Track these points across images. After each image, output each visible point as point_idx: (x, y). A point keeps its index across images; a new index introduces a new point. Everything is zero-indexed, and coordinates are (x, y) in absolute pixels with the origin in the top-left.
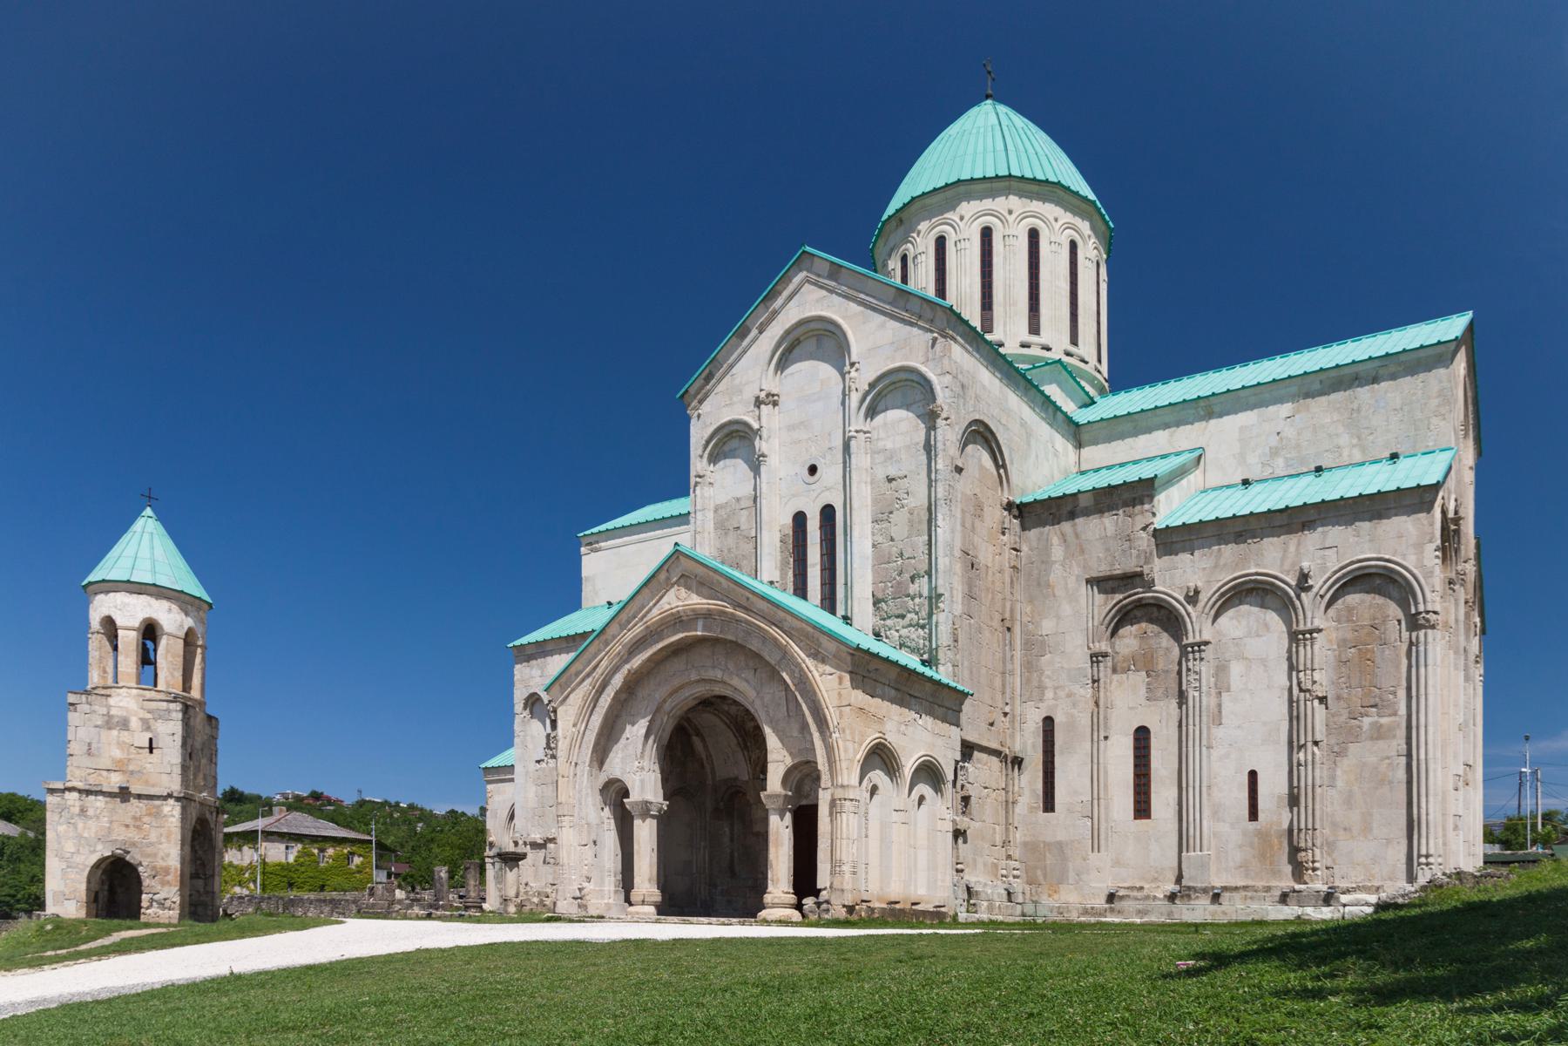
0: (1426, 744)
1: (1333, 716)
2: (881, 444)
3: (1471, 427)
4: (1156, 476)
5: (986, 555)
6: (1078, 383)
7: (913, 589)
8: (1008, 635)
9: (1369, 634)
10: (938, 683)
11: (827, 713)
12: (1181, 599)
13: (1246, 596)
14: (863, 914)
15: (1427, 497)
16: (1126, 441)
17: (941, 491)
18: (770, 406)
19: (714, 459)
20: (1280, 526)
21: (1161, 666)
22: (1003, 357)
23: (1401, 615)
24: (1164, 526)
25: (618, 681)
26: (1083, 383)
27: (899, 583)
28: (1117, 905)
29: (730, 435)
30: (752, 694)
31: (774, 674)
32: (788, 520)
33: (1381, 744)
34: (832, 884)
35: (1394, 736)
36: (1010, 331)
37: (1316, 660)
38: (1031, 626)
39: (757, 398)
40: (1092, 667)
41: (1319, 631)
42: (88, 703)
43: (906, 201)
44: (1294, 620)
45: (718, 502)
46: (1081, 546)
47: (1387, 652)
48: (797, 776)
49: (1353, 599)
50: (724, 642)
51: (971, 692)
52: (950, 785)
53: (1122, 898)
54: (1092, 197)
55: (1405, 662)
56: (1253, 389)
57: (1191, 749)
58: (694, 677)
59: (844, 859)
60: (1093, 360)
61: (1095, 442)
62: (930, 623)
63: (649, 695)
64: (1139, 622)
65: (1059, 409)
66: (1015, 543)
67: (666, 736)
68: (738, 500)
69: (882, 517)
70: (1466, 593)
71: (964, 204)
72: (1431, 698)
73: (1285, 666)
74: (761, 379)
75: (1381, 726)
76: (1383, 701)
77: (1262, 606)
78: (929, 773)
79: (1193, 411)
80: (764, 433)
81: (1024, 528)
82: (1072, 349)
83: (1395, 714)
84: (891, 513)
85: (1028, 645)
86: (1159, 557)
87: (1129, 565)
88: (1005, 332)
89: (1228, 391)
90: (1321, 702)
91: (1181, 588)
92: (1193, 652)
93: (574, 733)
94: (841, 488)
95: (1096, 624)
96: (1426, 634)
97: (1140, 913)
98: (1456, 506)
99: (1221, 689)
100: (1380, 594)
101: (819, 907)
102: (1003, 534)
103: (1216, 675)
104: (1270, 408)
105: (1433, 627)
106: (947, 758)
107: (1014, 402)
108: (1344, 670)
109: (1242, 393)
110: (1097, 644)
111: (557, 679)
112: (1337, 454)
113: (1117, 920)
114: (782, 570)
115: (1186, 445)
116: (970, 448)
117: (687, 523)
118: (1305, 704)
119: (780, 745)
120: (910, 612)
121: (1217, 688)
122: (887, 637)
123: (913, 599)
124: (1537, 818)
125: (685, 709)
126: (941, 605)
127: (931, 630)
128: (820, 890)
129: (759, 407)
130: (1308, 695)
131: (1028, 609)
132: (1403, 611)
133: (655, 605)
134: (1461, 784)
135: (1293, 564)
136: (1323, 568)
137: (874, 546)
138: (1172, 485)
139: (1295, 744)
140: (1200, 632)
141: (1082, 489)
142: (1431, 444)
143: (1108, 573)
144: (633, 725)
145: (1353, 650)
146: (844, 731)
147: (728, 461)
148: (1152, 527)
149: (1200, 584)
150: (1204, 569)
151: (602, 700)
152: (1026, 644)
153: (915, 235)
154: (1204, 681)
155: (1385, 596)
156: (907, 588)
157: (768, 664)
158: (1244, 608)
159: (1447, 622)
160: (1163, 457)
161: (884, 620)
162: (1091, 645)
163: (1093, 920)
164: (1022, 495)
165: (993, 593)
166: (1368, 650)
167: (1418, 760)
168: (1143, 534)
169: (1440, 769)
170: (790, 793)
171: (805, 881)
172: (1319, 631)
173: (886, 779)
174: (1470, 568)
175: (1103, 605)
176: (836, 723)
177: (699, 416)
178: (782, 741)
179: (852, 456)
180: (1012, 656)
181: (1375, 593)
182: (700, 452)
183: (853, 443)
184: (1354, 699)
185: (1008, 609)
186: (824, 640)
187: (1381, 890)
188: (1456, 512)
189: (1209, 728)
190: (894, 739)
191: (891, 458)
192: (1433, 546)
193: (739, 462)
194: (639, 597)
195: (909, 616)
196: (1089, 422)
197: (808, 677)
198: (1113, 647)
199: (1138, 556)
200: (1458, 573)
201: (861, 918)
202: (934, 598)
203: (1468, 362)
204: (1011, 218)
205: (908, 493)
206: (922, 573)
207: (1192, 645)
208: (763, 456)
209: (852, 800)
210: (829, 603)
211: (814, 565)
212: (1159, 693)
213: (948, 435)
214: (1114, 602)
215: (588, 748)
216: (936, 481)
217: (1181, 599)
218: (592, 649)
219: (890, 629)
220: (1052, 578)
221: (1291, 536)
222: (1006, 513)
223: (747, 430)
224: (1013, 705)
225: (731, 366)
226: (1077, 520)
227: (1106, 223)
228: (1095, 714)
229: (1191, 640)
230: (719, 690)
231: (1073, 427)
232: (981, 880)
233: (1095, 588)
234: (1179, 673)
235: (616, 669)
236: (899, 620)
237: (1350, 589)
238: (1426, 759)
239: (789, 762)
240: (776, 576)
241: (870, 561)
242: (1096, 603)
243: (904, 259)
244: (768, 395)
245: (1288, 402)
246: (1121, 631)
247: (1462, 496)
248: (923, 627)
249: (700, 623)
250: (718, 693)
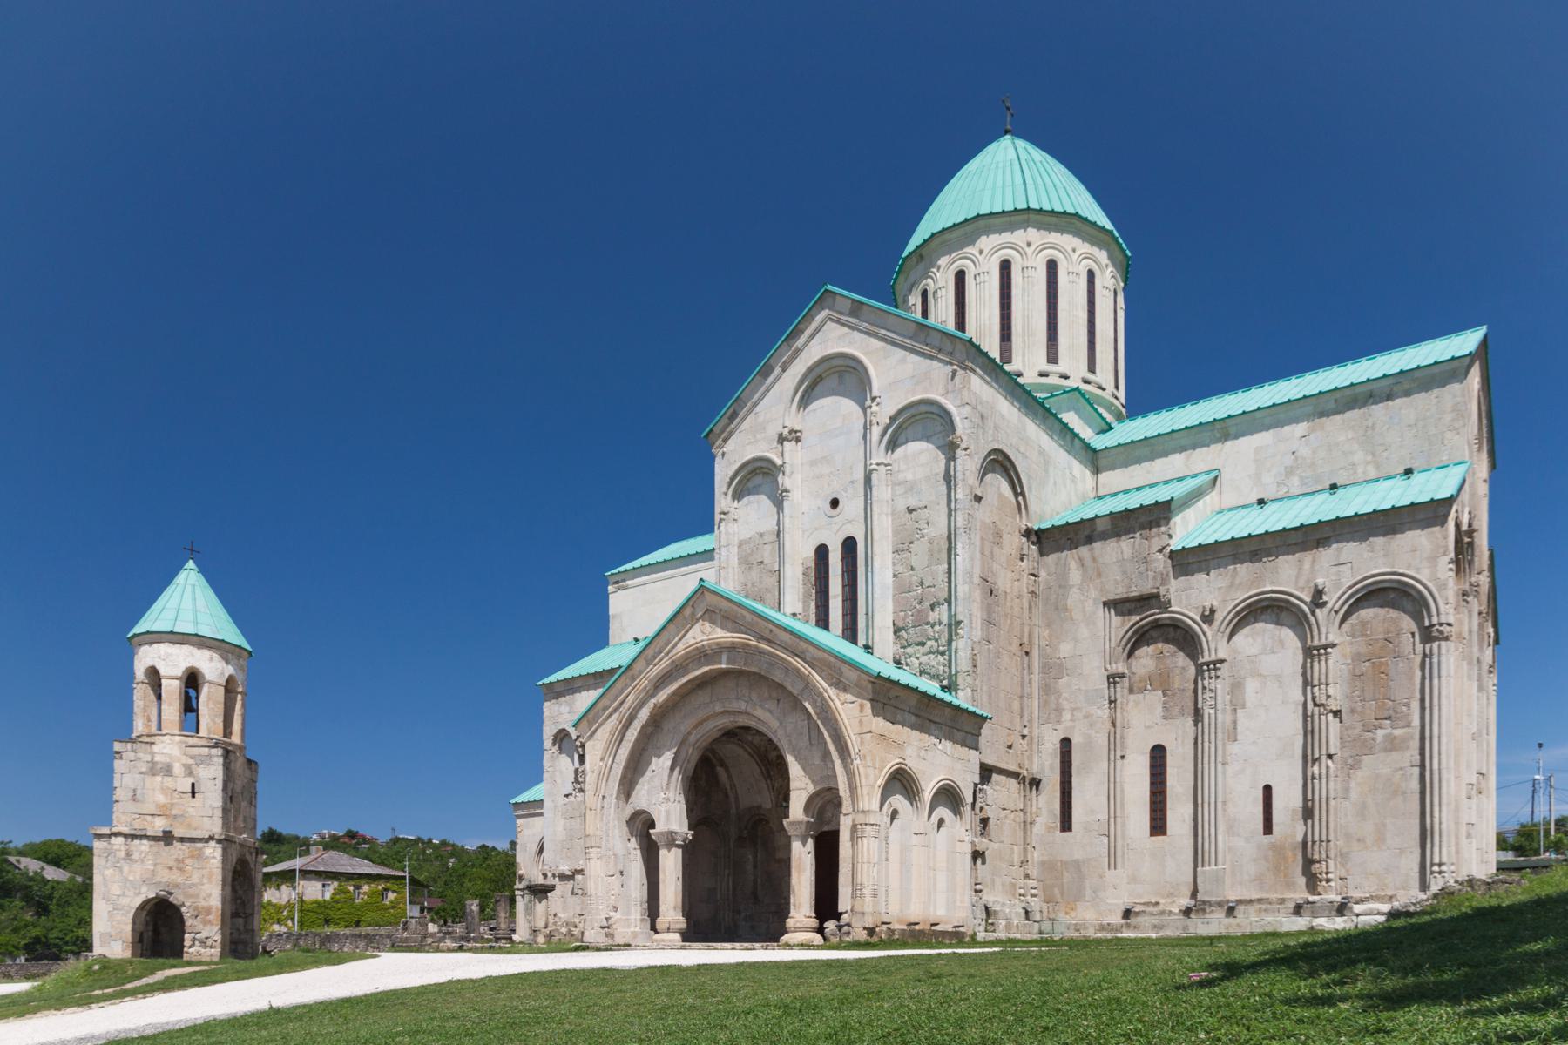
0: (1439, 754)
1: (1347, 729)
2: (901, 477)
3: (1485, 440)
4: (1172, 498)
5: (1004, 581)
6: (1096, 410)
7: (933, 617)
8: (1026, 658)
9: (1382, 648)
10: (958, 708)
11: (849, 741)
12: (1197, 618)
13: (1262, 612)
14: (883, 936)
15: (1441, 511)
16: (1143, 465)
17: (960, 520)
18: (793, 442)
19: (738, 495)
20: (1295, 544)
21: (1177, 685)
22: (1022, 386)
23: (1415, 628)
24: (1180, 548)
25: (644, 715)
26: (1101, 410)
27: (919, 611)
28: (1133, 921)
29: (754, 472)
30: (775, 724)
31: (797, 704)
32: (810, 553)
33: (1395, 755)
34: (853, 907)
35: (1408, 748)
36: (1028, 362)
37: (1331, 675)
38: (1049, 650)
39: (781, 435)
40: (1109, 688)
41: (1334, 646)
43: (926, 237)
44: (1309, 636)
45: (742, 538)
46: (1098, 569)
47: (1401, 665)
48: (818, 803)
49: (1367, 613)
50: (749, 673)
51: (990, 716)
52: (969, 808)
53: (1138, 913)
54: (1109, 226)
55: (1418, 674)
56: (1267, 410)
57: (1206, 766)
58: (718, 709)
59: (865, 882)
60: (1110, 387)
61: (1113, 468)
62: (949, 650)
63: (674, 728)
64: (1155, 642)
65: (1077, 436)
66: (1034, 568)
67: (692, 766)
68: (761, 535)
69: (902, 547)
70: (1480, 605)
71: (983, 238)
72: (1444, 709)
73: (1300, 681)
74: (784, 416)
75: (1395, 738)
76: (1397, 713)
77: (1278, 623)
78: (948, 796)
79: (1209, 434)
80: (787, 469)
81: (1042, 554)
82: (1090, 377)
83: (1408, 726)
84: (911, 543)
85: (1046, 668)
86: (1175, 578)
87: (1146, 587)
88: (1023, 362)
89: (1244, 412)
90: (1335, 716)
91: (1197, 608)
92: (1209, 670)
93: (601, 766)
94: (863, 520)
95: (1113, 645)
96: (1439, 646)
97: (1156, 927)
98: (1470, 519)
99: (1236, 705)
100: (1393, 607)
101: (840, 930)
102: (1022, 560)
103: (1231, 693)
104: (1285, 428)
105: (1446, 639)
106: (966, 781)
107: (1033, 430)
108: (1357, 683)
109: (1258, 415)
110: (1114, 666)
111: (585, 715)
112: (1351, 472)
113: (1132, 935)
114: (804, 602)
115: (1202, 467)
116: (989, 476)
117: (712, 559)
118: (1320, 719)
119: (802, 773)
120: (930, 639)
121: (1232, 705)
122: (907, 665)
123: (932, 627)
124: (1549, 824)
125: (710, 740)
126: (960, 631)
127: (950, 656)
128: (841, 914)
129: (782, 444)
130: (1322, 709)
131: (1046, 633)
132: (1417, 623)
133: (680, 640)
134: (1474, 793)
135: (1308, 581)
136: (1338, 584)
137: (895, 576)
138: (1189, 507)
139: (1309, 758)
140: (1216, 650)
141: (1100, 514)
142: (1445, 458)
143: (1125, 596)
144: (659, 758)
145: (1367, 664)
146: (865, 756)
147: (751, 498)
148: (1168, 550)
149: (1215, 604)
150: (1220, 588)
151: (628, 734)
152: (1044, 667)
153: (935, 270)
154: (1219, 698)
155: (1398, 609)
156: (927, 616)
157: (790, 694)
158: (1260, 625)
159: (1460, 634)
160: (1180, 479)
161: (904, 647)
162: (1108, 667)
163: (1109, 936)
164: (1040, 522)
165: (1011, 619)
166: (1382, 663)
167: (1431, 770)
168: (1160, 556)
169: (1453, 778)
170: (812, 820)
171: (826, 906)
172: (1334, 646)
173: (907, 803)
174: (1484, 580)
175: (1119, 627)
176: (857, 750)
177: (723, 454)
178: (804, 769)
179: (874, 489)
180: (1031, 679)
181: (1388, 606)
182: (724, 490)
183: (874, 476)
184: (1368, 712)
185: (1026, 635)
186: (845, 669)
187: (1394, 899)
188: (1470, 525)
189: (1224, 745)
190: (914, 765)
191: (911, 489)
192: (1447, 559)
193: (763, 498)
194: (665, 633)
195: (929, 643)
196: (1106, 448)
197: (829, 706)
198: (1129, 668)
199: (1155, 578)
200: (1471, 585)
201: (881, 940)
202: (954, 625)
203: (1482, 376)
204: (1029, 251)
205: (928, 523)
206: (942, 601)
207: (1208, 664)
208: (787, 491)
209: (872, 825)
210: (851, 633)
211: (836, 597)
212: (1176, 711)
213: (967, 466)
214: (1131, 623)
215: (615, 781)
216: (955, 510)
217: (1197, 618)
218: (619, 685)
219: (910, 657)
220: (1069, 602)
221: (1307, 553)
222: (1024, 540)
223: (770, 466)
224: (1031, 727)
225: (755, 405)
226: (1095, 545)
227: (1124, 252)
228: (1112, 734)
229: (1207, 659)
230: (743, 721)
231: (1091, 453)
232: (1001, 900)
233: (1112, 610)
234: (1195, 691)
235: (642, 704)
236: (919, 647)
237: (1365, 603)
238: (1439, 769)
239: (811, 789)
240: (799, 609)
241: (891, 592)
242: (1113, 625)
243: (924, 294)
244: (791, 431)
245: (1303, 422)
246: (1138, 652)
247: (1476, 509)
248: (942, 654)
249: (724, 657)
250: (741, 724)
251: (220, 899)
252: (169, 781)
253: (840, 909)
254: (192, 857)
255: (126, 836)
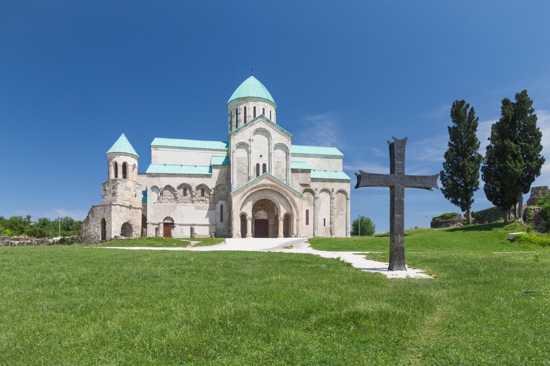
19: (237, 148)
21: (311, 200)
25: (248, 194)
29: (241, 144)
30: (277, 200)
42: (122, 183)
49: (339, 194)
58: (264, 195)
87: (307, 183)
147: (240, 149)
204: (268, 108)
212: (310, 204)
225: (243, 131)
230: (268, 198)
235: (248, 192)
239: (286, 212)
249: (269, 186)
251: (141, 223)
252: (130, 192)
253: (294, 233)
254: (135, 212)
255: (120, 205)
